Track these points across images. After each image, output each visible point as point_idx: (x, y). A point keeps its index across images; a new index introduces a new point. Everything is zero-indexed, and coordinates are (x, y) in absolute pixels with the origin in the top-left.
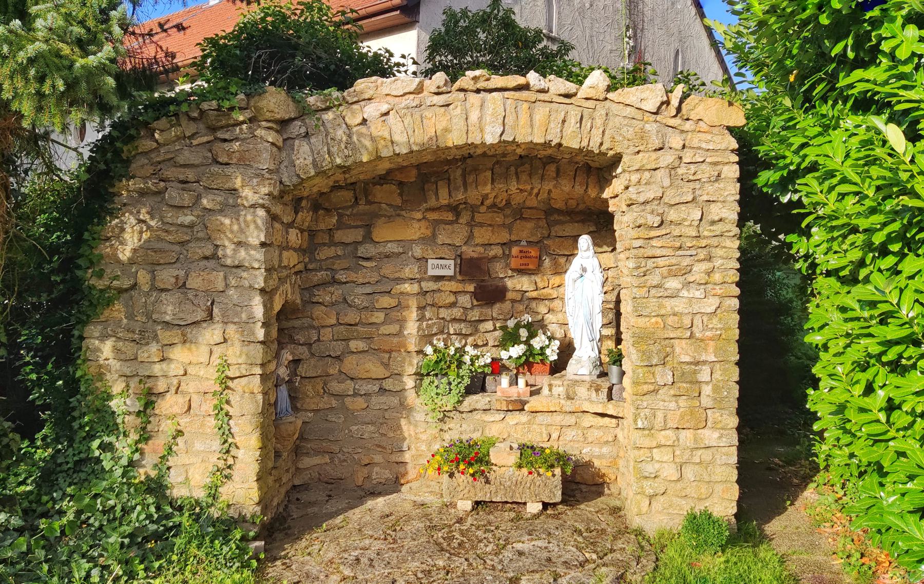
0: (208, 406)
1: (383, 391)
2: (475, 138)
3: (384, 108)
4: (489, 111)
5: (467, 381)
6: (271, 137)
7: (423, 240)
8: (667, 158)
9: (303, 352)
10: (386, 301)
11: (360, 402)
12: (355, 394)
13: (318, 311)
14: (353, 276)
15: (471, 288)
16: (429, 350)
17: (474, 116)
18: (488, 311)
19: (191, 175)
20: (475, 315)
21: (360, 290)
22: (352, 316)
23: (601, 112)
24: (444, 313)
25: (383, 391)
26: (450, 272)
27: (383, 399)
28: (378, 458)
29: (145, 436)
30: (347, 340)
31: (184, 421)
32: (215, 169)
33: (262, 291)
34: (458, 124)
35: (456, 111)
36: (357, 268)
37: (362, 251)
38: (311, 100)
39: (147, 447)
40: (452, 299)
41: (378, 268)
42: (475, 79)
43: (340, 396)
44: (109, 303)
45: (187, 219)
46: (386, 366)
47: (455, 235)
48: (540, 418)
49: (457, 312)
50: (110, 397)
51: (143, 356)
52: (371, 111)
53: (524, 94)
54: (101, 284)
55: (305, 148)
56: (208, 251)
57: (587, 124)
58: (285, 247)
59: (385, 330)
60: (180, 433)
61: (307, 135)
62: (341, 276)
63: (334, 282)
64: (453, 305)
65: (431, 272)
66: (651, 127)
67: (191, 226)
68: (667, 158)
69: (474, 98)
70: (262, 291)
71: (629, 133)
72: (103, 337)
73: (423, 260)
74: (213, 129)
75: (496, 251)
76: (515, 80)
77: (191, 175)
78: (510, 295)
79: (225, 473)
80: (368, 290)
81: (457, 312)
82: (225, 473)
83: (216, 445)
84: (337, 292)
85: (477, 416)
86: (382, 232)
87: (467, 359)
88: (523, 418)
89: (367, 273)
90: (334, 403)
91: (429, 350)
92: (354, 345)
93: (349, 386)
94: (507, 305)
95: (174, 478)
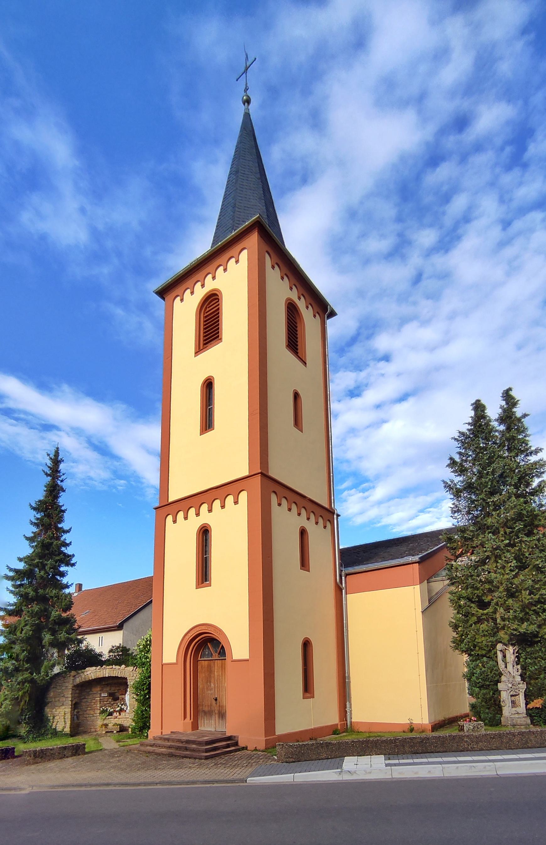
0: (63, 717)
1: (93, 716)
2: (104, 676)
3: (90, 672)
4: (107, 671)
5: (108, 714)
6: (72, 678)
7: (100, 690)
8: (134, 678)
9: (80, 710)
10: (94, 701)
11: (89, 718)
12: (89, 717)
13: (82, 703)
14: (88, 697)
15: (112, 698)
16: (101, 709)
17: (104, 673)
18: (115, 702)
19: (60, 684)
20: (112, 703)
21: (89, 699)
22: (88, 704)
23: (124, 671)
24: (105, 703)
25: (93, 716)
26: (107, 696)
27: (93, 717)
28: (92, 727)
29: (53, 722)
30: (87, 708)
31: (59, 720)
32: (64, 684)
33: (71, 701)
34: (102, 674)
35: (102, 672)
36: (89, 696)
37: (90, 693)
38: (79, 672)
39: (53, 724)
40: (107, 700)
41: (93, 696)
42: (104, 667)
43: (86, 717)
44: (48, 704)
45: (60, 691)
46: (94, 712)
47: (108, 689)
48: (120, 719)
49: (108, 702)
50: (48, 717)
51: (53, 711)
52: (88, 673)
53: (112, 669)
54: (47, 701)
55: (78, 679)
56: (63, 695)
57: (122, 673)
58: (76, 693)
59: (94, 706)
60: (58, 722)
61: (78, 677)
62: (86, 697)
63: (85, 698)
64: (107, 701)
65: (102, 696)
66: (131, 673)
67: (60, 692)
68: (134, 678)
69: (104, 670)
70: (71, 701)
71: (128, 674)
72: (48, 708)
73: (100, 694)
74: (64, 678)
75: (117, 691)
76: (111, 667)
77: (60, 684)
78: (120, 699)
79: (65, 727)
80: (91, 699)
81: (108, 702)
82: (65, 727)
83: (64, 723)
84: (85, 700)
85: (109, 719)
86: (93, 690)
87: (108, 710)
88: (117, 719)
89: (91, 696)
90: (85, 718)
91: (101, 709)
92: (89, 709)
93: (88, 716)
94: (119, 701)
95: (57, 728)
